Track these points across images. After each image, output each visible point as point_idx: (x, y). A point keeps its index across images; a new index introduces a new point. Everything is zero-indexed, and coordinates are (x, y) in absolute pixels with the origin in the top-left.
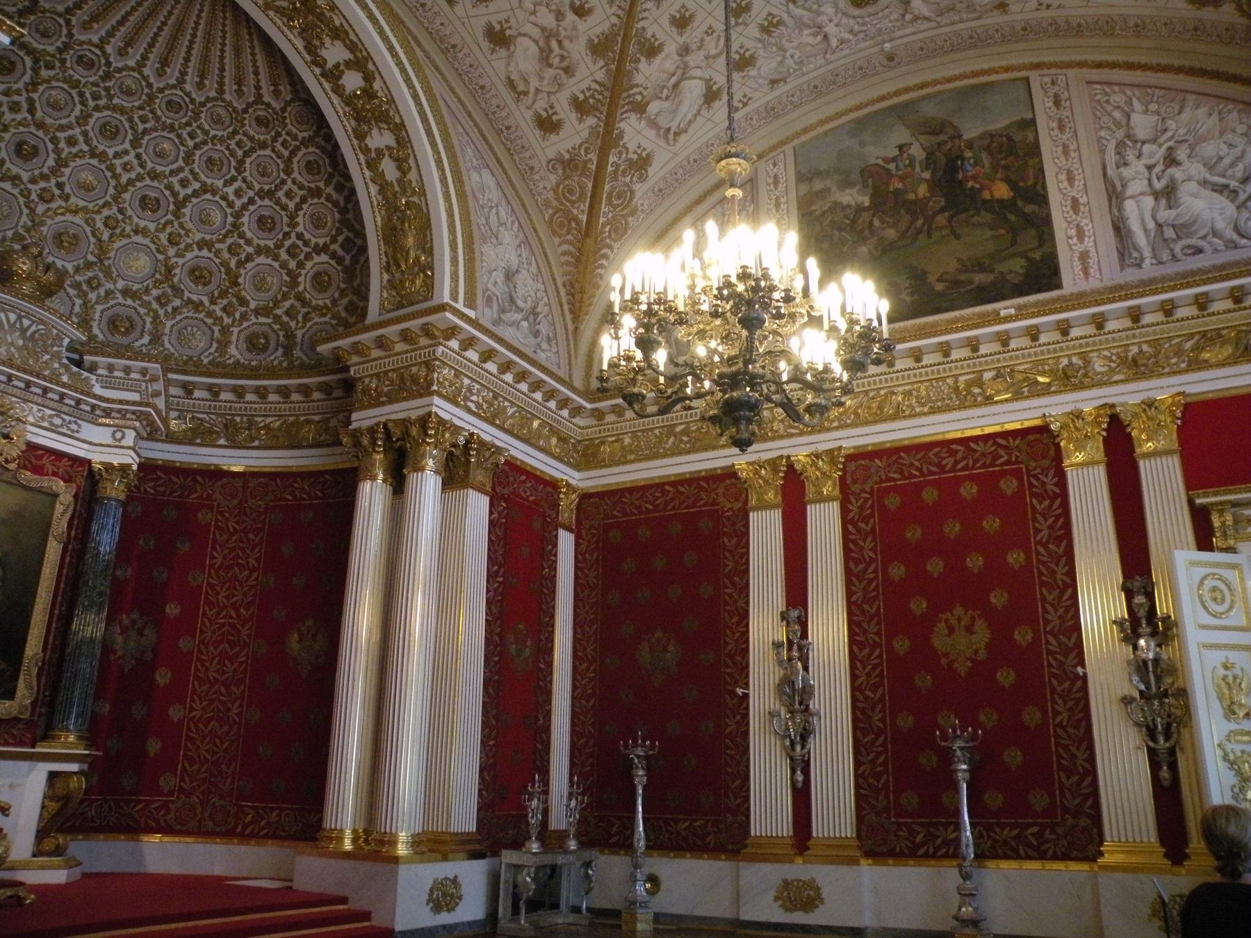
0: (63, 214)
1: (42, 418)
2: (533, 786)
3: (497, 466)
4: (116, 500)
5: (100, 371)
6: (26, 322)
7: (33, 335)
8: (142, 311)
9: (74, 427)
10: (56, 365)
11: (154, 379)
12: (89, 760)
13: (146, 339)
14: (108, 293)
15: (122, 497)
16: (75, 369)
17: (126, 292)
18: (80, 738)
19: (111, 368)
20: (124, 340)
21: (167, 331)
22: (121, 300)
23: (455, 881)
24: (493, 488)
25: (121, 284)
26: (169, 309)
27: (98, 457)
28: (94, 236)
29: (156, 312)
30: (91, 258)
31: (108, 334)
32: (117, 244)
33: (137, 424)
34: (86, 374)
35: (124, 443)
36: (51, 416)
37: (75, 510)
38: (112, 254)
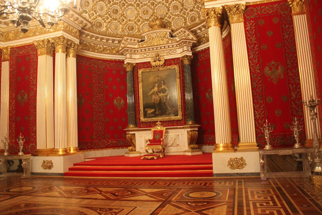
0: (172, 3)
1: (167, 53)
2: (265, 125)
3: (244, 11)
4: (187, 64)
5: (177, 36)
6: (158, 34)
7: (160, 37)
8: (195, 13)
9: (175, 51)
10: (168, 40)
11: (185, 32)
12: (198, 127)
13: (198, 18)
14: (187, 13)
15: (187, 63)
16: (172, 38)
17: (191, 11)
18: (193, 123)
19: (177, 34)
20: (194, 22)
21: (201, 14)
22: (191, 13)
23: (242, 159)
24: (245, 18)
25: (189, 10)
26: (200, 9)
27: (179, 56)
28: (179, 3)
29: (197, 11)
30: (181, 8)
31: (191, 23)
32: (184, 2)
33: (185, 44)
34: (174, 38)
35: (184, 50)
36: (169, 52)
37: (180, 70)
38: (184, 4)
